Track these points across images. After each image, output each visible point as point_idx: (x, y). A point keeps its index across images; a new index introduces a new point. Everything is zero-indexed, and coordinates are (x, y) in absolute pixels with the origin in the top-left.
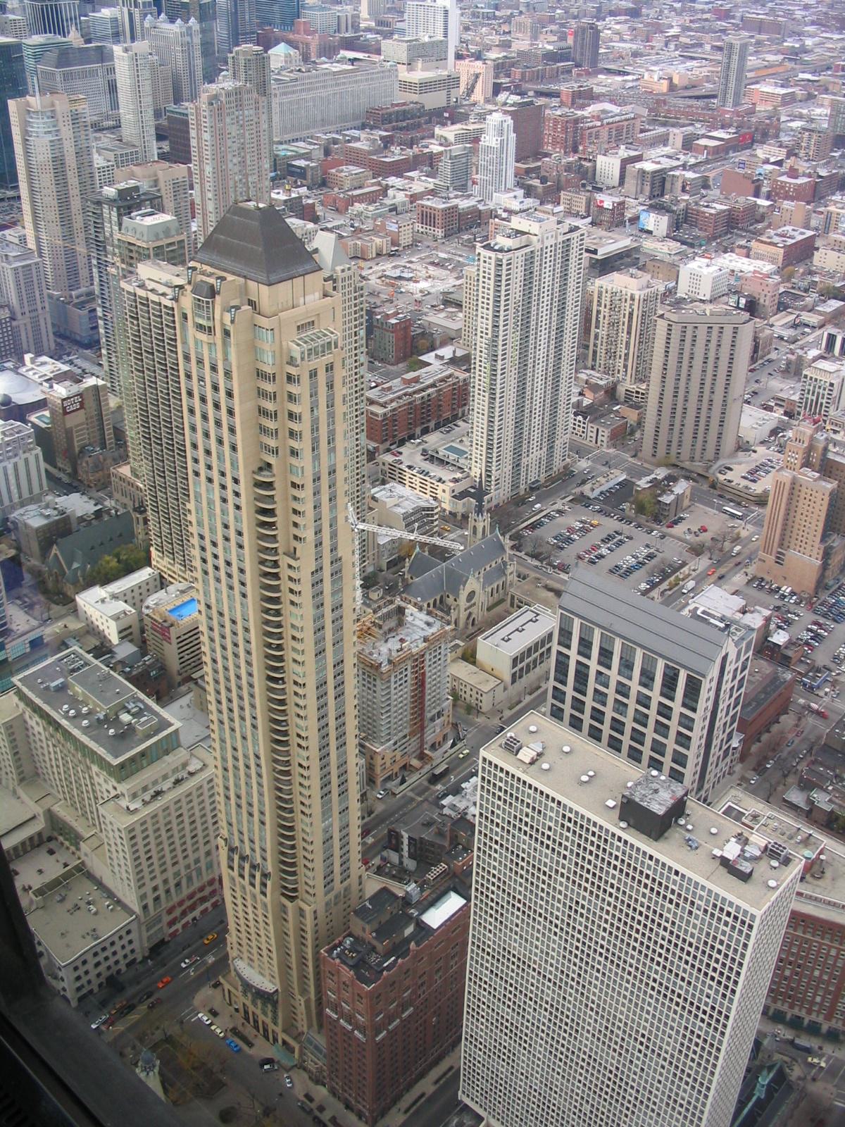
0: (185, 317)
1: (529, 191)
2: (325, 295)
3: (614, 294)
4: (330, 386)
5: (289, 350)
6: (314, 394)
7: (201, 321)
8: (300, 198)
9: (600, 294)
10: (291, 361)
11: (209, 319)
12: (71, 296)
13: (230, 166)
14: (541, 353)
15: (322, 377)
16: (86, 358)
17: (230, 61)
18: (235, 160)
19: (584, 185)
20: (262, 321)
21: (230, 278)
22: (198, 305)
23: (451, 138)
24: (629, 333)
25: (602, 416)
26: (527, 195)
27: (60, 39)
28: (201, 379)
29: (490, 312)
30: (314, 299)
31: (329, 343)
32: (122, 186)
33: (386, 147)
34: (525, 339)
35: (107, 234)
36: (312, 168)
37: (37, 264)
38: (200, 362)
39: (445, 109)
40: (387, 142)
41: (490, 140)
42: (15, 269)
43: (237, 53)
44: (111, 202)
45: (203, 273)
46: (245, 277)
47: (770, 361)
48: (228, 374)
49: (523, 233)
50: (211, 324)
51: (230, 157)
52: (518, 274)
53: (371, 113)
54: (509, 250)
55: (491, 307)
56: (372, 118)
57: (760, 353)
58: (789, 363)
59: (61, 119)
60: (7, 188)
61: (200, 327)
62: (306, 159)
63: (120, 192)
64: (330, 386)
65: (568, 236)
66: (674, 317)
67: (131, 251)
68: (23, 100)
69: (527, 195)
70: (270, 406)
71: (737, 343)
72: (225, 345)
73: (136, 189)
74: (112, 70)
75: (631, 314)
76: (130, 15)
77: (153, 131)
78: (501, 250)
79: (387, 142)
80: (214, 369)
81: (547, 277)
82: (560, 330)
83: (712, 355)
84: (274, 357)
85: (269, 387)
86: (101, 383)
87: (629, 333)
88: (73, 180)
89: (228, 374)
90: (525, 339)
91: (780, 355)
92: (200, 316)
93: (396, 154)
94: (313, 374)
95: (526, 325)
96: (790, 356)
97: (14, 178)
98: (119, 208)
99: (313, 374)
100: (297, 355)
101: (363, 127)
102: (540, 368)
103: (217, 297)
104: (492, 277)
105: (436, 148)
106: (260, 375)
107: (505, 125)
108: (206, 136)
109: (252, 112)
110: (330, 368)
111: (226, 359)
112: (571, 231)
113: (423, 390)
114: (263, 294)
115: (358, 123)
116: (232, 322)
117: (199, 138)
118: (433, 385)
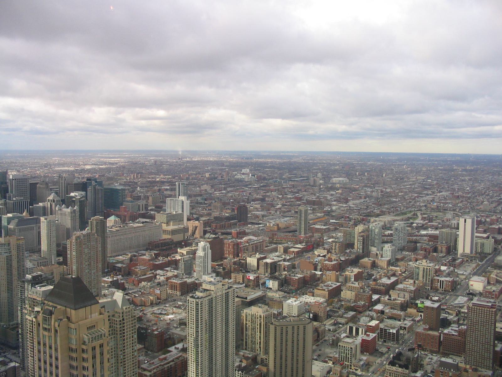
0: (39, 324)
1: (218, 274)
2: (100, 314)
3: (252, 315)
4: (102, 354)
5: (83, 338)
6: (94, 357)
7: (45, 326)
8: (118, 280)
9: (246, 316)
10: (84, 343)
11: (49, 325)
12: (9, 325)
13: (84, 266)
14: (219, 343)
15: (98, 351)
16: (14, 354)
17: (90, 223)
18: (86, 263)
19: (241, 270)
20: (72, 326)
21: (59, 307)
22: (45, 319)
23: (185, 253)
24: (260, 332)
25: (250, 371)
26: (217, 276)
28: (45, 353)
29: (194, 325)
30: (96, 316)
31: (101, 335)
32: (35, 274)
33: (156, 258)
34: (211, 337)
36: (124, 267)
38: (45, 345)
39: (182, 241)
40: (157, 256)
41: (200, 253)
43: (93, 220)
44: (29, 281)
45: (48, 305)
46: (66, 307)
47: (325, 341)
48: (56, 350)
49: (207, 290)
50: (50, 327)
51: (84, 262)
52: (206, 308)
53: (150, 244)
54: (201, 298)
55: (194, 323)
56: (150, 246)
57: (320, 337)
58: (333, 341)
61: (45, 329)
62: (122, 263)
64: (102, 354)
65: (227, 291)
66: (277, 324)
67: (34, 302)
69: (217, 276)
70: (74, 364)
71: (306, 332)
72: (56, 336)
73: (41, 276)
74: (40, 228)
75: (260, 324)
76: (51, 205)
77: (55, 252)
78: (198, 298)
79: (157, 256)
80: (50, 347)
81: (219, 308)
82: (227, 332)
83: (295, 339)
84: (76, 341)
85: (74, 355)
86: (17, 365)
87: (260, 332)
89: (56, 350)
90: (211, 337)
91: (329, 337)
92: (45, 324)
93: (161, 260)
94: (94, 348)
95: (211, 331)
96: (333, 338)
99: (94, 348)
100: (87, 340)
101: (147, 250)
102: (219, 349)
103: (53, 316)
104: (195, 310)
105: (178, 257)
106: (71, 350)
107: (206, 247)
108: (74, 253)
109: (94, 243)
110: (101, 346)
111: (56, 343)
112: (229, 288)
113: (168, 363)
114: (73, 313)
115: (145, 248)
116: (59, 326)
117: (71, 254)
118: (173, 361)
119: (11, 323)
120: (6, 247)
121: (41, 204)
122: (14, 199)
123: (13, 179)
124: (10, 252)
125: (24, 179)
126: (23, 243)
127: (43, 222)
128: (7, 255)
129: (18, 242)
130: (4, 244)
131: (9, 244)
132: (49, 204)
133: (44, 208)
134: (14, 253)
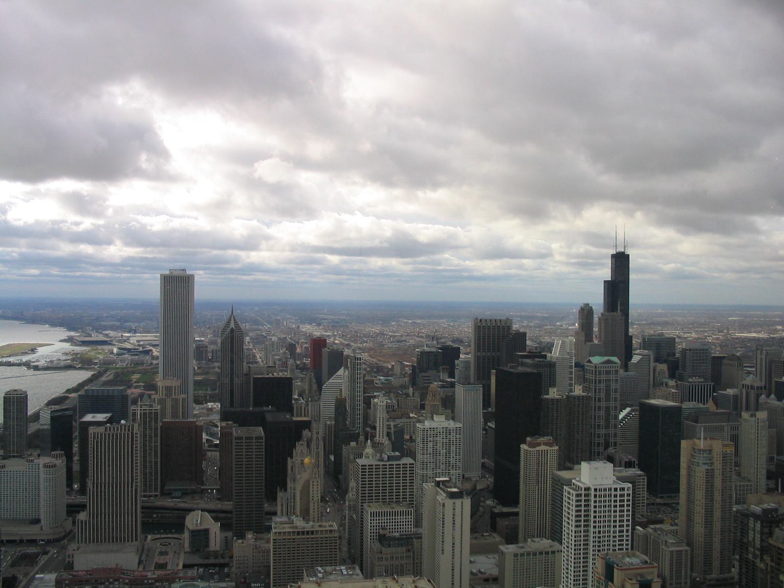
12: (705, 579)
27: (701, 405)
32: (765, 506)
35: (750, 539)
37: (686, 551)
42: (672, 552)
44: (756, 517)
59: (715, 456)
60: (657, 497)
63: (764, 511)
68: (691, 441)
76: (747, 394)
77: (764, 472)
88: (717, 497)
97: (677, 491)
98: (762, 522)
119: (708, 577)
120: (705, 455)
121: (730, 392)
122: (690, 380)
123: (687, 350)
124: (712, 463)
125: (703, 350)
126: (731, 451)
127: (745, 420)
128: (707, 468)
129: (724, 450)
130: (703, 450)
131: (710, 451)
132: (744, 391)
133: (735, 397)
134: (718, 466)
